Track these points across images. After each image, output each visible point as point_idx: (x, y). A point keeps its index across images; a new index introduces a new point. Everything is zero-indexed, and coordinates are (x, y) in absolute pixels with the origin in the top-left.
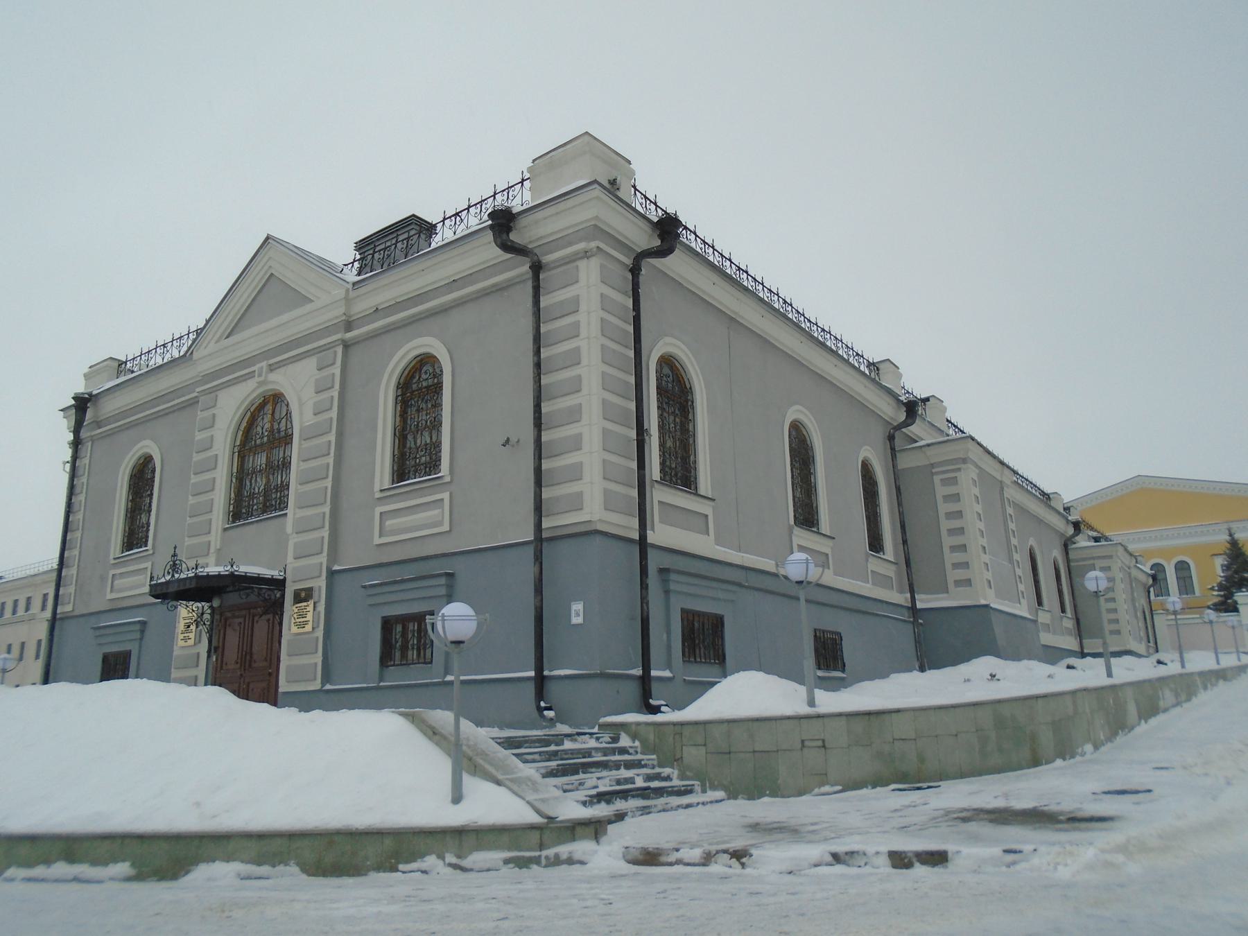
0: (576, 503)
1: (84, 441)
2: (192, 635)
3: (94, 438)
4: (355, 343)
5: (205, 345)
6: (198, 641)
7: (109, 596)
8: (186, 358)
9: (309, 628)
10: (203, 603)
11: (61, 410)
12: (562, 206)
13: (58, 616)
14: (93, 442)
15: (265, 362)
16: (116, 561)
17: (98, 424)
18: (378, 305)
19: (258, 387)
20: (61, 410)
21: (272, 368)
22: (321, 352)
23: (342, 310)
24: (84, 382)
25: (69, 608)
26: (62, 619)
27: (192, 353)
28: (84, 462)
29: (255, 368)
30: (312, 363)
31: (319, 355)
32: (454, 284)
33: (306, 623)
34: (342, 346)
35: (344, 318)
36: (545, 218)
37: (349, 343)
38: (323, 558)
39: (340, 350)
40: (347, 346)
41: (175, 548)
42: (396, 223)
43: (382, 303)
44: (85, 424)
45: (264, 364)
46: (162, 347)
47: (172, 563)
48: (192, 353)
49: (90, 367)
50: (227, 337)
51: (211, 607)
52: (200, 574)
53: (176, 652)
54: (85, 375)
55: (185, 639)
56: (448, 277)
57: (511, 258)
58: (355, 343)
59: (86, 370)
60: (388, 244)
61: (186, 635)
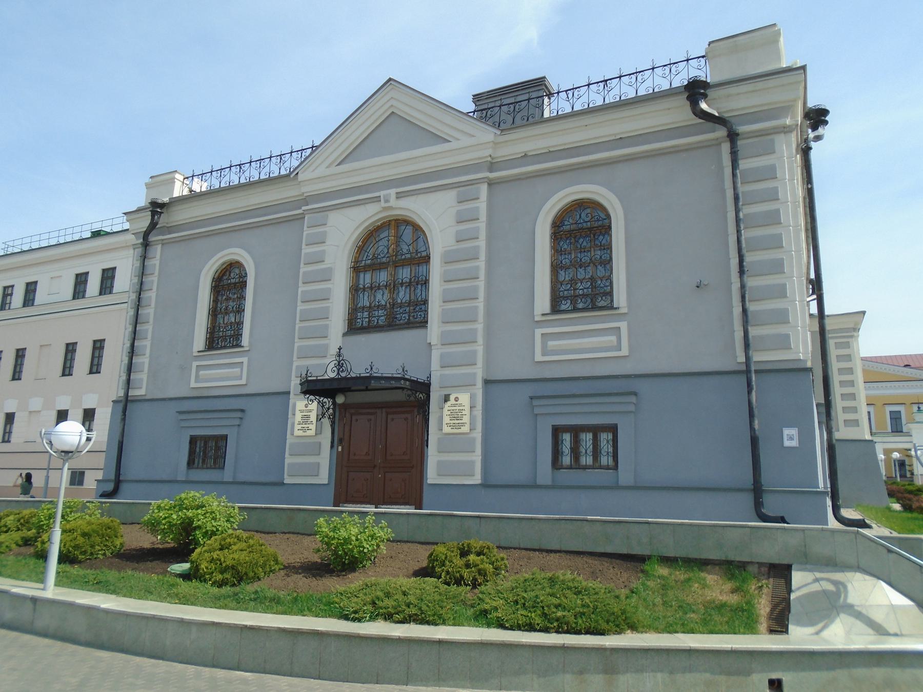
0: (784, 342)
1: (151, 244)
2: (313, 427)
3: (164, 242)
4: (498, 183)
5: (311, 168)
6: (319, 431)
8: (290, 177)
9: (466, 429)
10: (329, 399)
12: (760, 85)
13: (129, 399)
14: (163, 244)
17: (170, 229)
18: (526, 152)
19: (380, 212)
21: (399, 196)
22: (459, 187)
24: (145, 190)
26: (132, 401)
27: (297, 173)
28: (155, 262)
29: (382, 193)
30: (451, 195)
31: (458, 189)
32: (621, 142)
33: (463, 424)
34: (486, 184)
35: (489, 159)
36: (739, 94)
37: (492, 182)
39: (484, 188)
40: (491, 184)
42: (519, 84)
43: (530, 151)
44: (157, 227)
45: (393, 192)
46: (238, 167)
47: (336, 362)
48: (297, 173)
49: (151, 177)
50: (338, 165)
51: (334, 403)
52: (375, 375)
53: (290, 440)
54: (146, 185)
55: (303, 429)
56: (615, 135)
57: (704, 122)
58: (498, 183)
59: (148, 180)
60: (519, 99)
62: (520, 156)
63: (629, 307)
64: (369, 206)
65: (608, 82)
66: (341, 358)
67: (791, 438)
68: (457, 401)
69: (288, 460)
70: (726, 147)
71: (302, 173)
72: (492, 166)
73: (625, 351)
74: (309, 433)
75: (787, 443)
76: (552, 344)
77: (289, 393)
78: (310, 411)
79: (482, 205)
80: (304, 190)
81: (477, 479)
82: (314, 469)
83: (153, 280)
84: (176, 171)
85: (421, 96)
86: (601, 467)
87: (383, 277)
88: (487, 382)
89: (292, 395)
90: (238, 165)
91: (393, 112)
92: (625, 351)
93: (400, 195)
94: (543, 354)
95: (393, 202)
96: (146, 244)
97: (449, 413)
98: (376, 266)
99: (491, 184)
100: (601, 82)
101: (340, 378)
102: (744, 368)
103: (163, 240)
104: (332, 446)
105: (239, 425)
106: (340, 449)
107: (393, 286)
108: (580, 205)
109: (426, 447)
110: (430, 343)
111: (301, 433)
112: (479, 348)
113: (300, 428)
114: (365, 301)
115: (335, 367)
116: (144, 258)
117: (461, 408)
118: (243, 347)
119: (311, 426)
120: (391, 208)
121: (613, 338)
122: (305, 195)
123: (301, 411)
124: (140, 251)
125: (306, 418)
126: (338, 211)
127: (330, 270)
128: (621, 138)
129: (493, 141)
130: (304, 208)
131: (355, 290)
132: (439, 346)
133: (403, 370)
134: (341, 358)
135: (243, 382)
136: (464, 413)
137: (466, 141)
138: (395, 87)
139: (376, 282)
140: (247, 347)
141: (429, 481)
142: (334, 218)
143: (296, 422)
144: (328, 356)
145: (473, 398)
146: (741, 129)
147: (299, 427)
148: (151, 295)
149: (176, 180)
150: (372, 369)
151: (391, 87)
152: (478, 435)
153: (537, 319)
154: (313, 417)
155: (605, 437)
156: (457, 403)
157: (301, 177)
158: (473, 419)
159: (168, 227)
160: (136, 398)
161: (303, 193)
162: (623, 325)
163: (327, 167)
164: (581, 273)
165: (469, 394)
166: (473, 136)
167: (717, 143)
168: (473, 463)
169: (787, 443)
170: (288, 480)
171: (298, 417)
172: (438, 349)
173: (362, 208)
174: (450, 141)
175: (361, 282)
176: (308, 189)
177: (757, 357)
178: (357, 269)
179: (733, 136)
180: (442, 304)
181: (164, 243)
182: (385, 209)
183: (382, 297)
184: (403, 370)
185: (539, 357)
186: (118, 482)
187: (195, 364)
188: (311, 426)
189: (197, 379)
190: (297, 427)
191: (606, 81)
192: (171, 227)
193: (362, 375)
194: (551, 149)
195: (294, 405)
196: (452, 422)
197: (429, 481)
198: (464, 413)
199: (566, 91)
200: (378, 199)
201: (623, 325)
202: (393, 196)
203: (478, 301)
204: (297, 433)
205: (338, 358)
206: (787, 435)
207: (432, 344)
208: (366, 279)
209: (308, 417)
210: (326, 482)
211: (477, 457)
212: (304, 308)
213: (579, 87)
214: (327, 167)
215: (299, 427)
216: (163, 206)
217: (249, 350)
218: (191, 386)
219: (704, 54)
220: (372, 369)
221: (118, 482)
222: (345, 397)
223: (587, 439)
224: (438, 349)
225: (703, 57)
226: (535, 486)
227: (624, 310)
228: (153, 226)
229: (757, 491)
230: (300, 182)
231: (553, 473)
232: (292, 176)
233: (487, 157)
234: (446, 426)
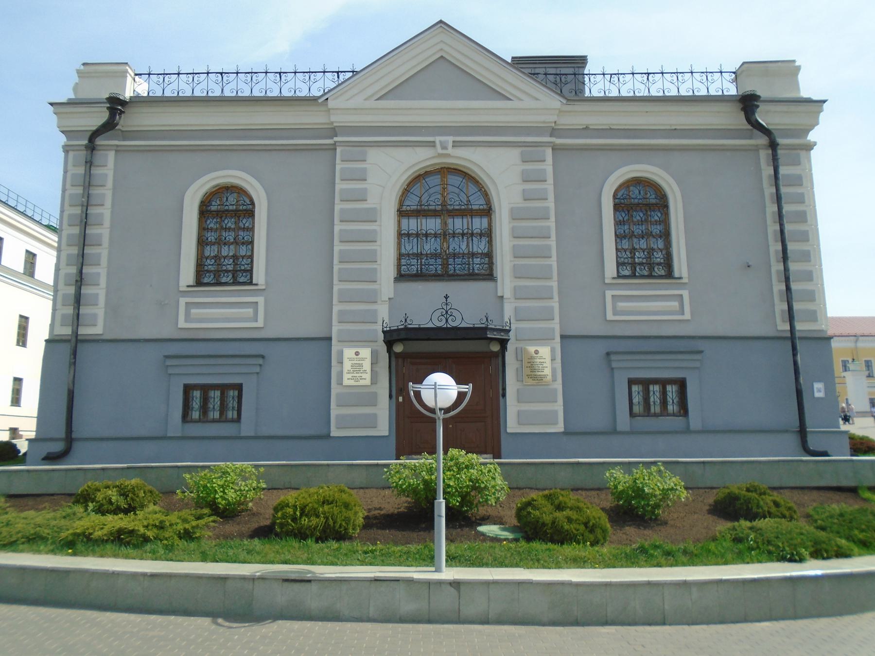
4: (560, 149)
7: (182, 324)
11: (51, 104)
13: (79, 338)
14: (116, 151)
15: (452, 137)
16: (190, 289)
17: (127, 135)
19: (434, 157)
20: (51, 104)
21: (456, 144)
23: (554, 118)
25: (96, 330)
27: (327, 99)
29: (438, 139)
30: (513, 155)
31: (524, 149)
38: (555, 326)
39: (549, 152)
40: (555, 148)
41: (446, 297)
43: (591, 125)
45: (450, 139)
49: (84, 64)
53: (335, 389)
56: (671, 125)
58: (560, 149)
61: (353, 375)
62: (581, 127)
63: (689, 278)
64: (419, 150)
65: (651, 76)
66: (449, 307)
67: (819, 391)
68: (536, 354)
69: (335, 411)
70: (764, 155)
71: (334, 99)
72: (554, 132)
73: (687, 316)
74: (362, 383)
75: (817, 395)
76: (621, 305)
77: (330, 339)
78: (363, 359)
79: (548, 166)
80: (333, 119)
81: (560, 428)
83: (105, 193)
84: (127, 63)
85: (474, 45)
86: (668, 415)
87: (432, 224)
88: (562, 337)
89: (334, 342)
90: (219, 73)
91: (442, 57)
92: (687, 316)
93: (458, 144)
94: (614, 314)
95: (450, 150)
96: (91, 147)
98: (420, 213)
99: (555, 148)
100: (645, 74)
101: (449, 328)
103: (117, 146)
104: (391, 397)
105: (258, 373)
106: (401, 399)
107: (444, 235)
108: (638, 182)
109: (501, 398)
110: (502, 297)
111: (352, 383)
112: (555, 304)
113: (351, 377)
114: (410, 247)
115: (443, 315)
116: (89, 164)
117: (542, 361)
118: (256, 285)
119: (364, 376)
120: (448, 156)
121: (675, 304)
122: (335, 124)
123: (350, 359)
124: (83, 154)
125: (357, 368)
126: (382, 149)
127: (373, 211)
128: (675, 129)
129: (559, 109)
130: (336, 139)
131: (401, 235)
132: (513, 300)
134: (449, 307)
135: (260, 323)
136: (545, 365)
137: (528, 103)
138: (444, 31)
139: (468, 229)
140: (262, 285)
141: (509, 430)
142: (375, 156)
143: (345, 370)
145: (553, 351)
146: (781, 141)
147: (350, 376)
148: (104, 212)
149: (128, 75)
150: (487, 320)
151: (441, 29)
152: (558, 386)
153: (607, 281)
154: (367, 365)
155: (672, 391)
156: (536, 355)
157: (331, 104)
158: (554, 371)
159: (122, 131)
160: (87, 338)
161: (332, 123)
162: (685, 294)
163: (365, 100)
164: (643, 244)
165: (550, 348)
166: (539, 100)
167: (756, 149)
168: (556, 412)
169: (817, 395)
170: (334, 433)
171: (347, 365)
172: (511, 302)
173: (409, 150)
174: (511, 100)
175: (450, 227)
176: (338, 119)
177: (799, 326)
178: (402, 213)
179: (773, 146)
180: (512, 259)
181: (118, 150)
182: (440, 155)
183: (431, 246)
185: (610, 316)
186: (69, 440)
187: (183, 301)
188: (364, 376)
189: (188, 318)
190: (346, 376)
191: (649, 74)
192: (126, 131)
193: (476, 326)
194: (612, 127)
195: (341, 354)
197: (509, 430)
198: (545, 365)
199: (611, 75)
200: (432, 144)
201: (685, 294)
202: (450, 144)
203: (551, 259)
204: (346, 382)
205: (445, 307)
206: (817, 388)
207: (505, 297)
208: (412, 225)
209: (361, 365)
210: (387, 433)
211: (559, 407)
212: (342, 248)
213: (624, 74)
214: (365, 100)
215: (350, 376)
216: (123, 103)
217: (264, 289)
218: (179, 326)
219: (734, 70)
220: (487, 320)
221: (69, 440)
222: (404, 346)
223: (655, 388)
224: (511, 302)
225: (734, 73)
226: (614, 432)
227: (685, 280)
228: (108, 126)
229: (803, 432)
230: (329, 110)
231: (630, 420)
232: (320, 101)
233: (551, 122)
234: (527, 377)
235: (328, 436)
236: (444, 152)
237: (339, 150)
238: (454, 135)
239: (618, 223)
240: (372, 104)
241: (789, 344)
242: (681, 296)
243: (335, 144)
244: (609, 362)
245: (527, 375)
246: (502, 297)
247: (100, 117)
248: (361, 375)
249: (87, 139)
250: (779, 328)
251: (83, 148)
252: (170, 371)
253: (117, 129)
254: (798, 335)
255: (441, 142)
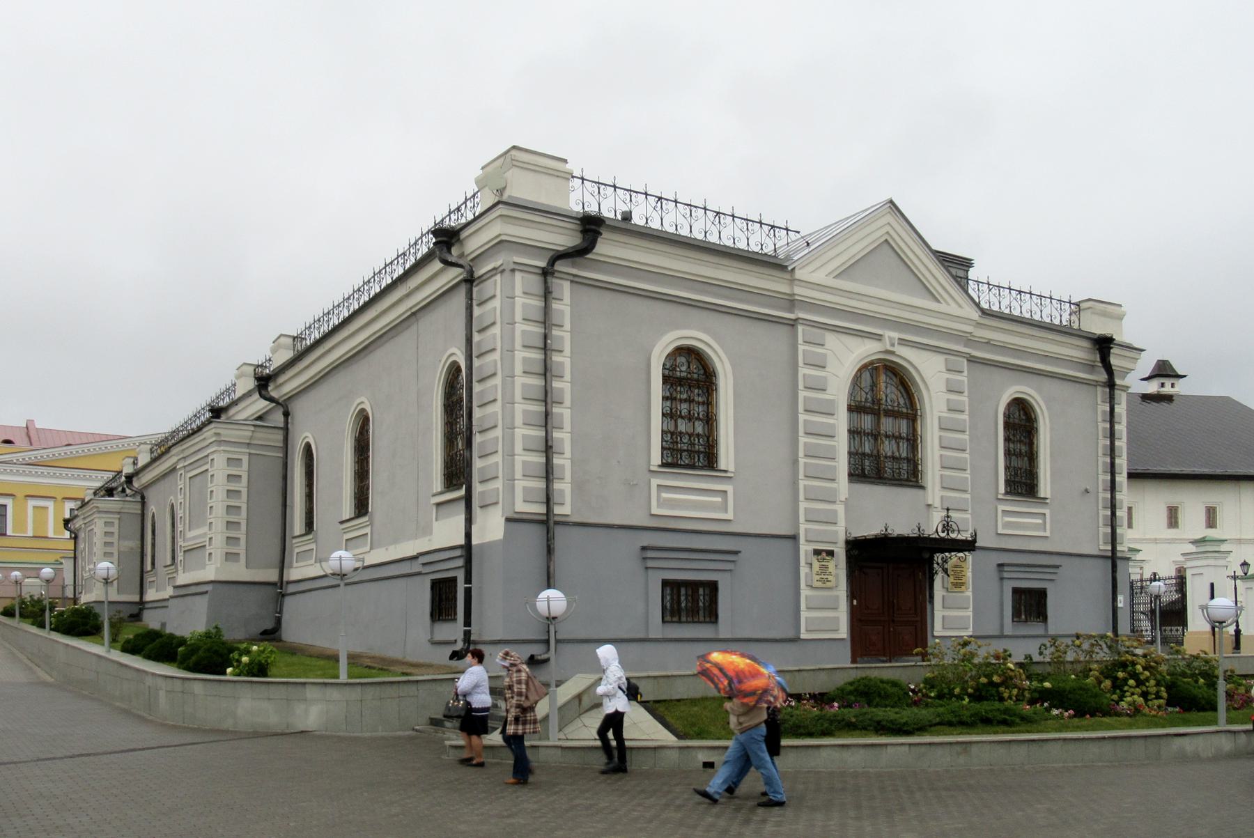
45: (896, 335)
61: (821, 576)
71: (800, 269)
73: (1047, 534)
80: (797, 290)
82: (833, 625)
97: (953, 573)
102: (1110, 554)
106: (855, 602)
120: (893, 353)
122: (797, 297)
133: (919, 529)
137: (953, 309)
144: (838, 503)
147: (818, 577)
167: (1095, 384)
184: (919, 529)
188: (830, 578)
196: (955, 581)
215: (818, 577)
235: (796, 640)
236: (891, 349)
237: (800, 328)
238: (900, 331)
239: (1007, 440)
240: (831, 282)
241: (1109, 563)
242: (1045, 514)
243: (796, 320)
244: (1001, 571)
245: (952, 583)
246: (929, 506)
247: (566, 239)
248: (828, 577)
249: (547, 261)
250: (1102, 548)
251: (540, 271)
252: (650, 564)
253: (586, 258)
254: (1119, 555)
255: (889, 337)
